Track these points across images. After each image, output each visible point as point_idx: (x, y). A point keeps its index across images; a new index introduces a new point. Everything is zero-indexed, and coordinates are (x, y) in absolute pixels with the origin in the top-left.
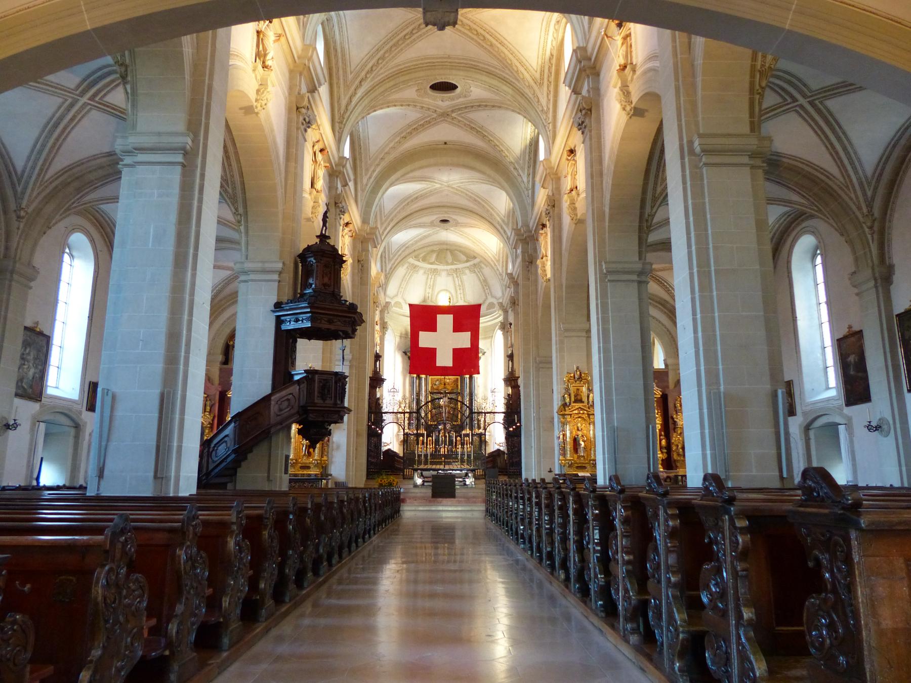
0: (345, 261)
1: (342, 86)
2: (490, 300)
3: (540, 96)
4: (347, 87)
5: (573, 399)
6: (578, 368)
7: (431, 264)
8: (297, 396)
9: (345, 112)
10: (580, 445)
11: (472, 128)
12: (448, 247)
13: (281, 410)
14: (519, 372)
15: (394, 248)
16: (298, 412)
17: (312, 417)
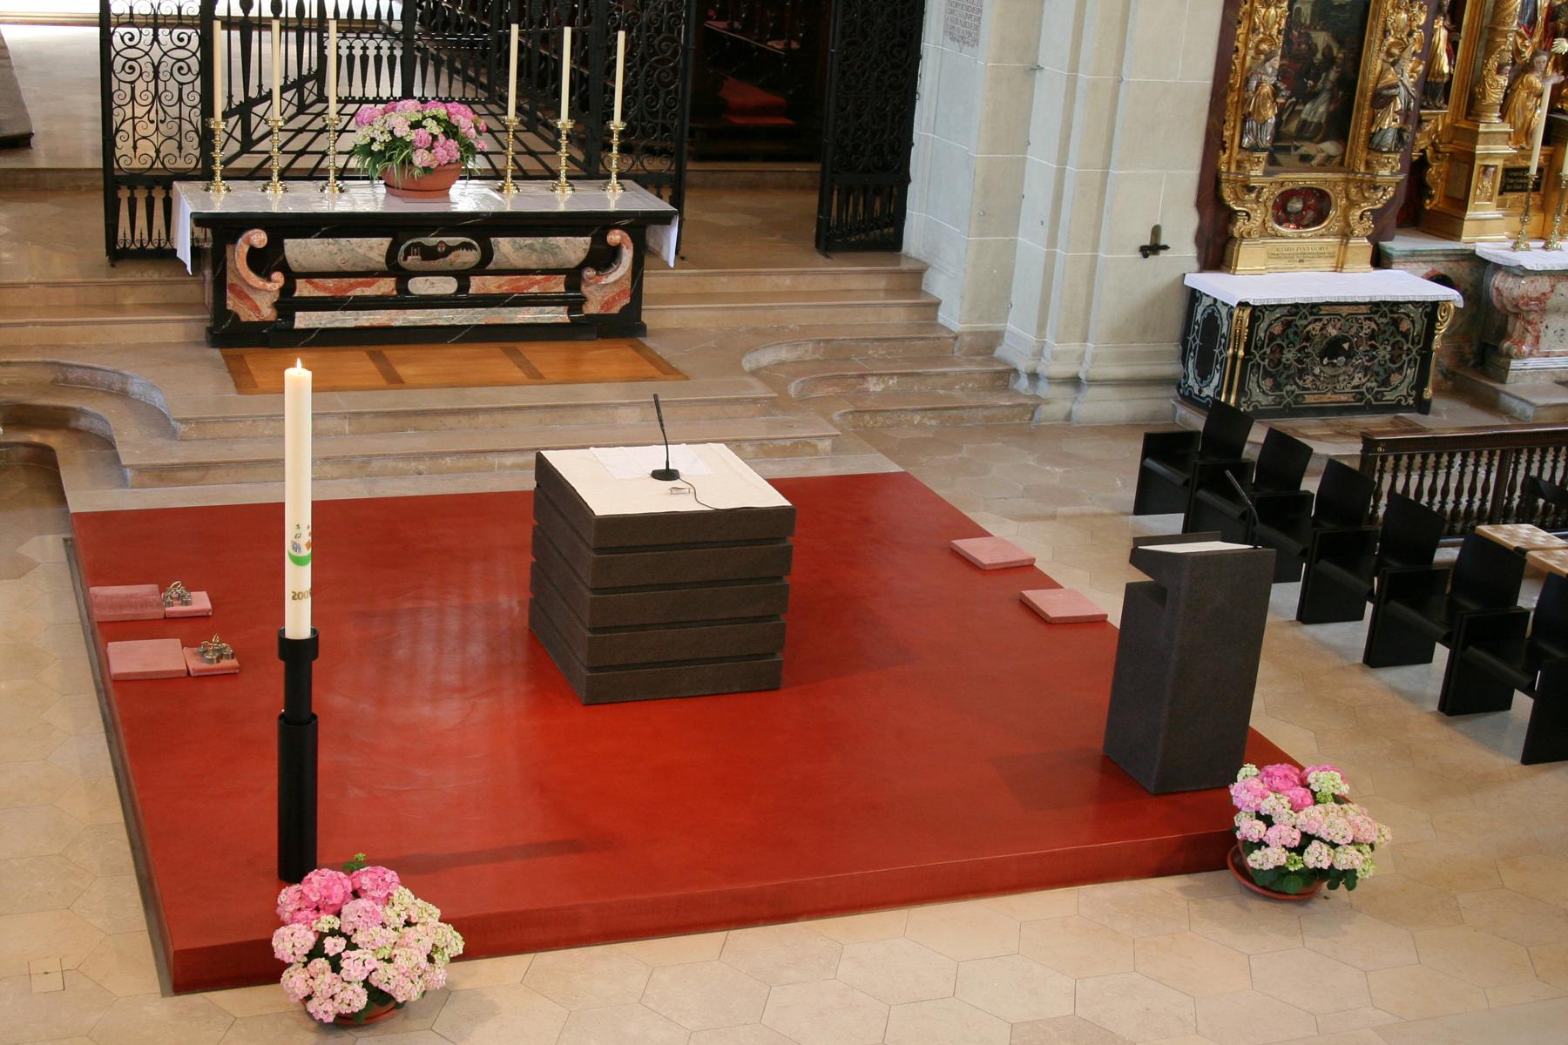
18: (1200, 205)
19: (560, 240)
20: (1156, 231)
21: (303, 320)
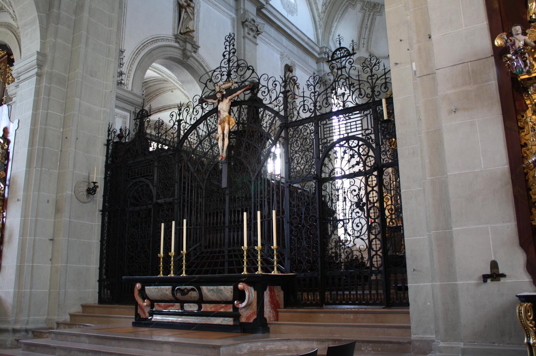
19: (222, 287)
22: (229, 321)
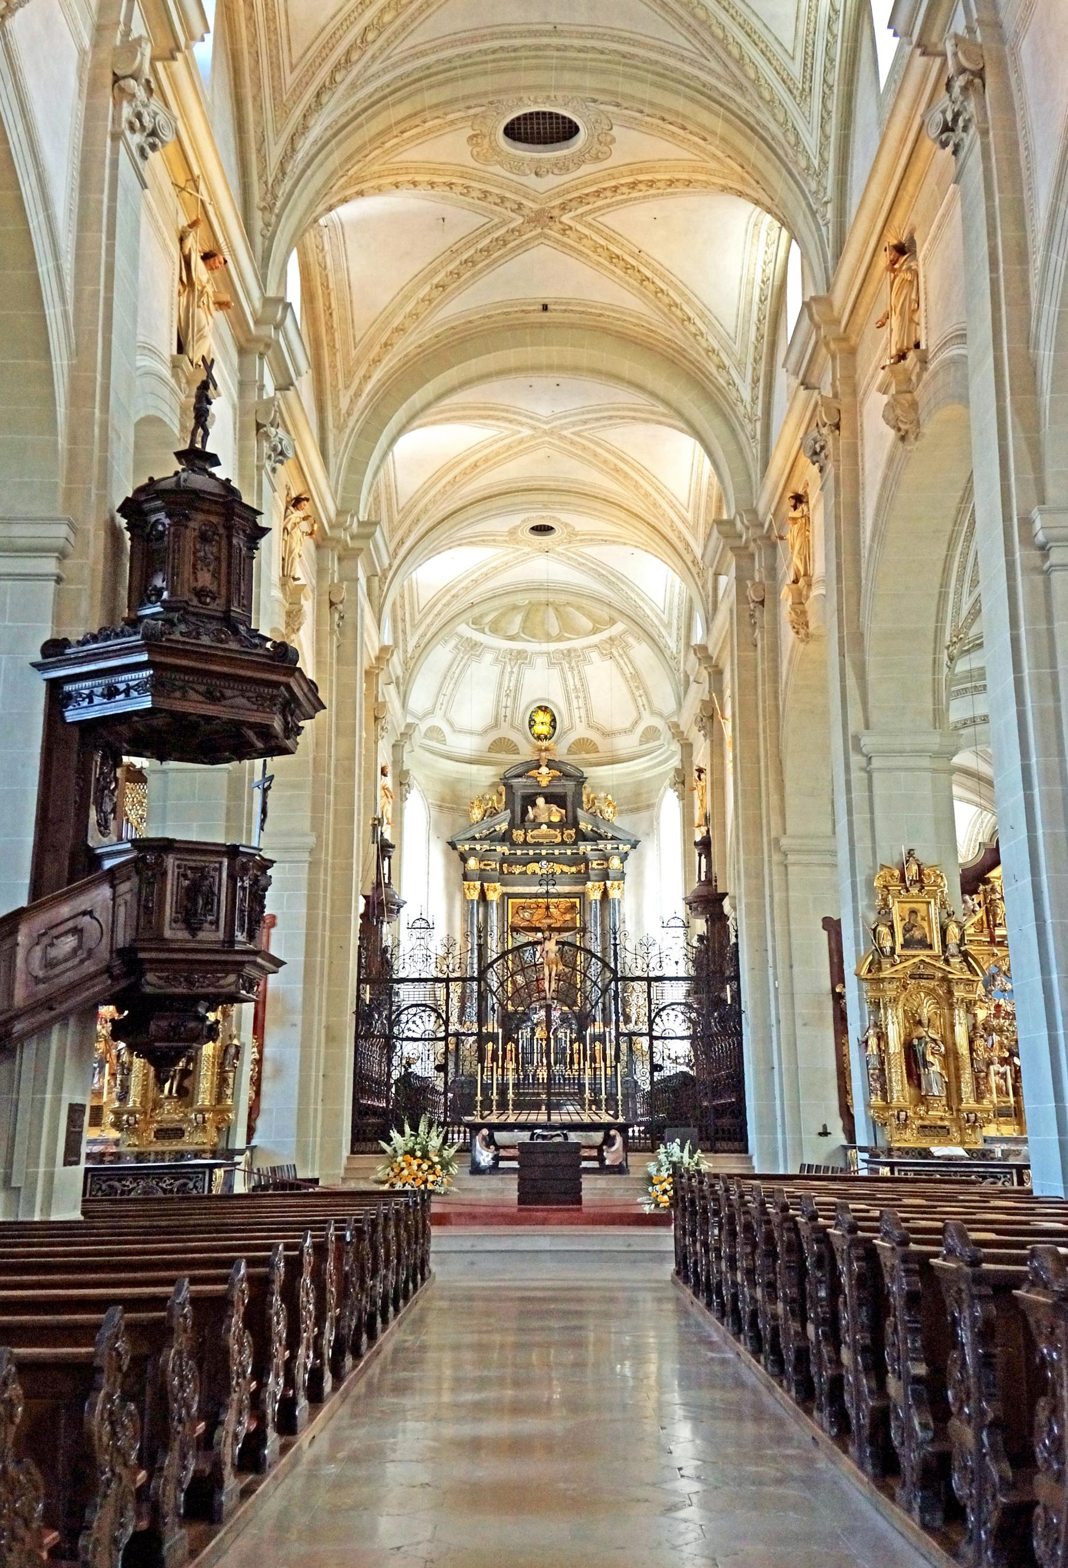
0: (264, 531)
1: (268, 105)
2: (649, 720)
3: (801, 126)
4: (283, 109)
5: (900, 940)
6: (910, 853)
7: (512, 638)
8: (104, 917)
9: (278, 181)
10: (926, 1065)
11: (613, 258)
12: (551, 597)
13: (50, 964)
14: (733, 884)
15: (425, 597)
16: (108, 970)
17: (152, 982)
18: (841, 1116)
20: (825, 1126)
21: (502, 1164)
22: (595, 1164)
